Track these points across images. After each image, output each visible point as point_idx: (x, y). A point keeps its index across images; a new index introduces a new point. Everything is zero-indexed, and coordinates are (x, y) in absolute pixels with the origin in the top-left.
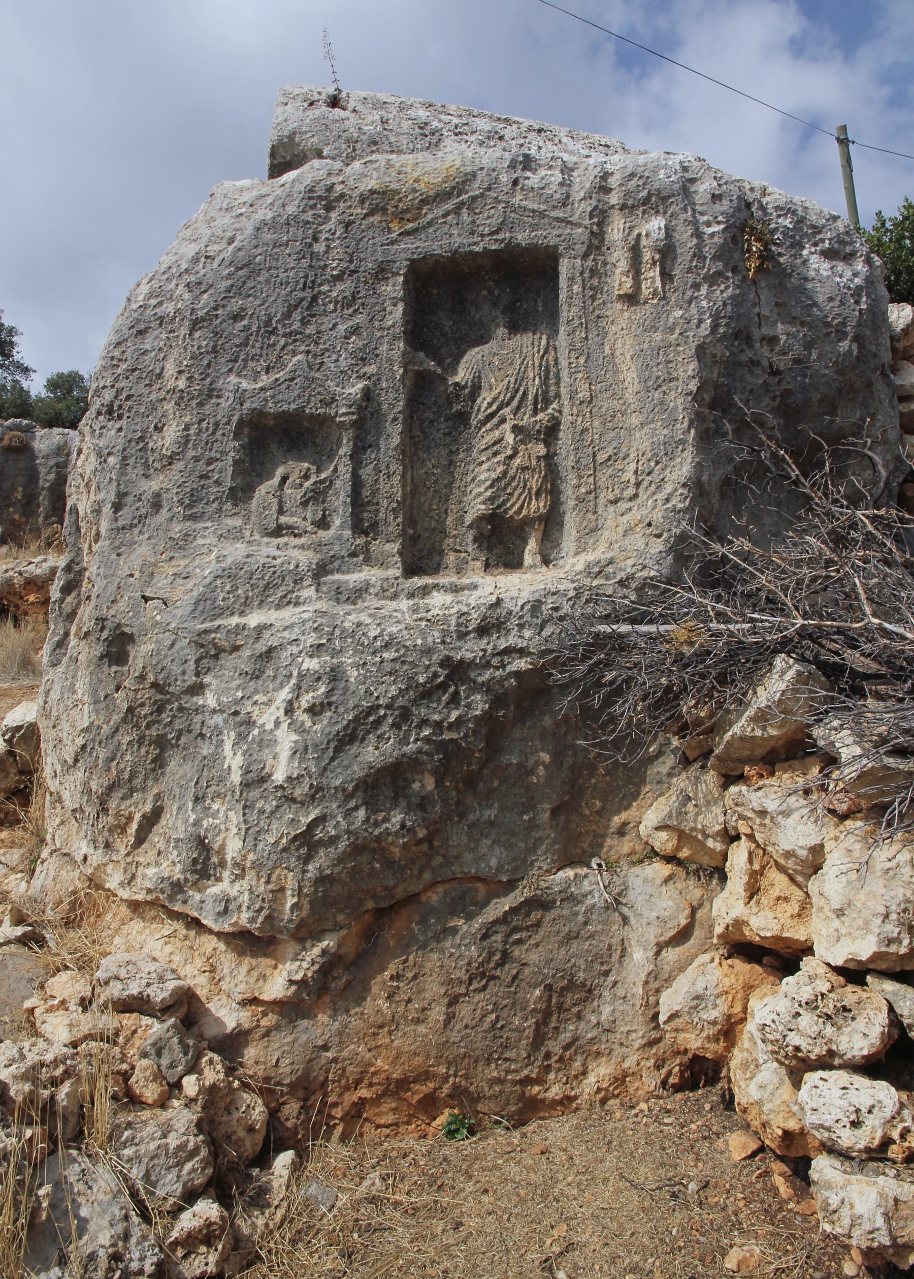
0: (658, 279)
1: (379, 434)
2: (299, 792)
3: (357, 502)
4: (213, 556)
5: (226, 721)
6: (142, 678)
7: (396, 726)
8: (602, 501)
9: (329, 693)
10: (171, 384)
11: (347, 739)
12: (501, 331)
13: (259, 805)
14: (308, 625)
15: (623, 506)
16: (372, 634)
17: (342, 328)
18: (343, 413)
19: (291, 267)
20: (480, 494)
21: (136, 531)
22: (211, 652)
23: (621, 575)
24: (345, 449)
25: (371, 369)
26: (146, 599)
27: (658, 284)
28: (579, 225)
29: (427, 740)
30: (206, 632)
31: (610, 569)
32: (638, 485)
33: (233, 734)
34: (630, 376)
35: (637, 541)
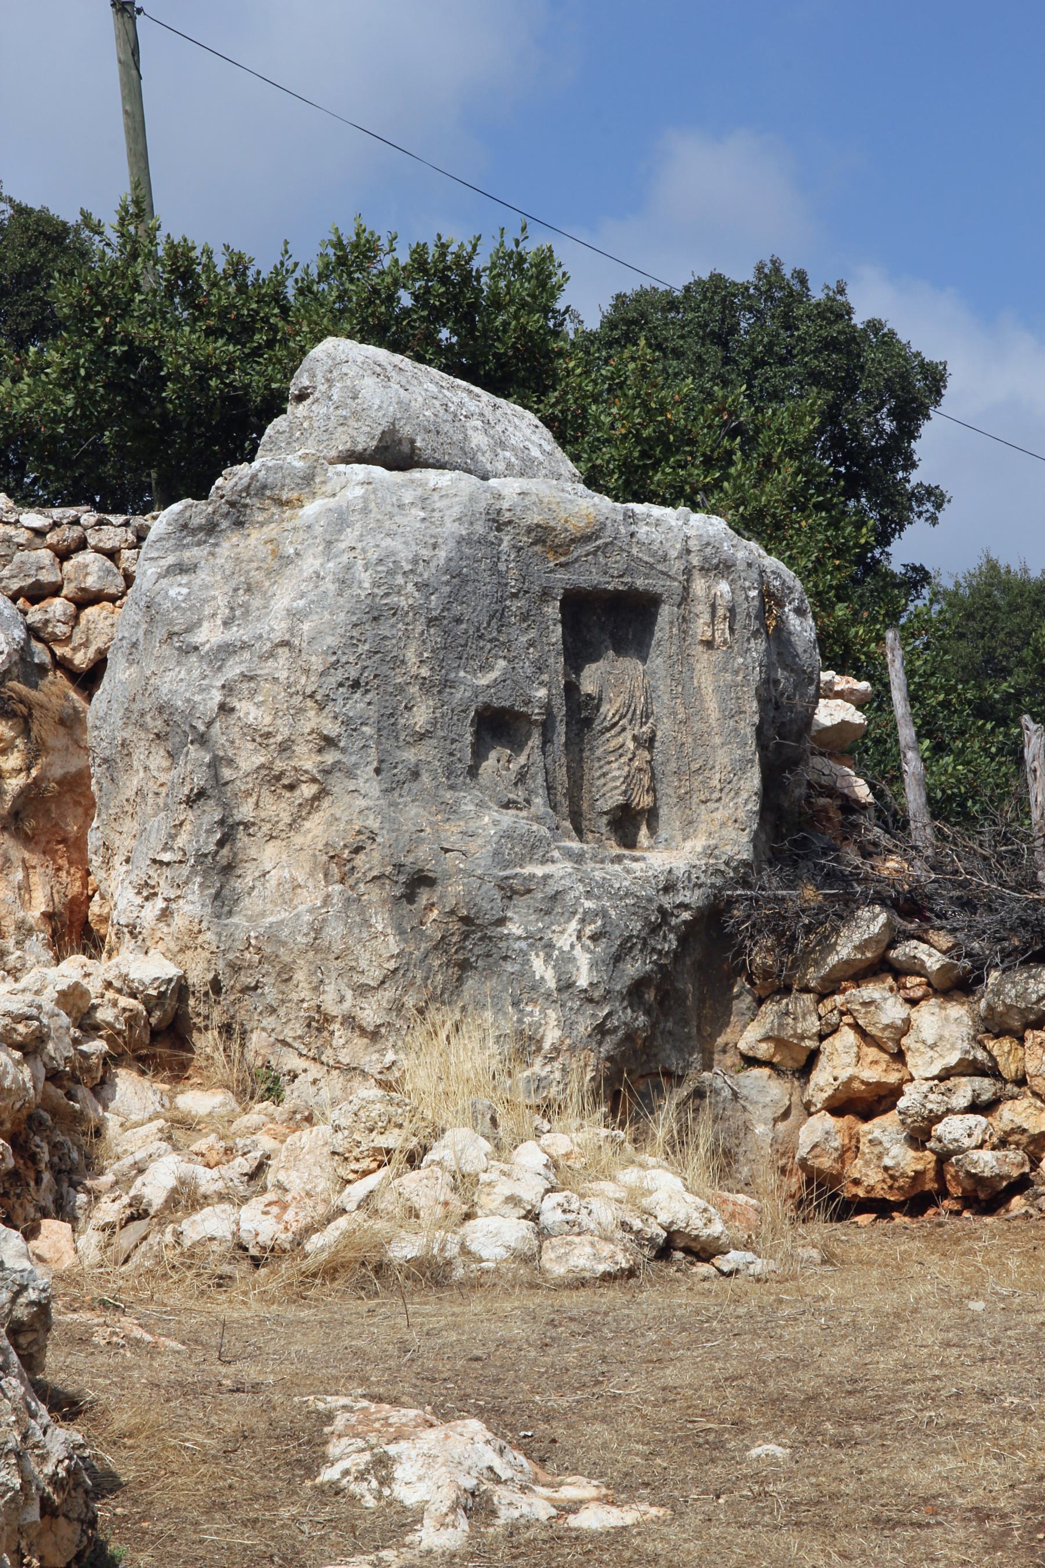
0: (727, 631)
1: (553, 732)
2: (596, 994)
3: (550, 788)
4: (487, 819)
5: (531, 946)
6: (452, 912)
7: (641, 951)
8: (695, 800)
9: (604, 925)
10: (414, 671)
11: (617, 959)
12: (611, 653)
13: (569, 1004)
14: (574, 877)
15: (711, 805)
16: (617, 886)
17: (524, 639)
18: (536, 713)
19: (487, 584)
20: (616, 788)
21: (396, 794)
22: (510, 892)
23: (725, 857)
24: (535, 740)
25: (545, 677)
26: (447, 851)
27: (727, 635)
28: (675, 579)
29: (655, 963)
30: (507, 878)
31: (717, 852)
32: (721, 790)
33: (541, 954)
34: (712, 705)
35: (730, 832)
